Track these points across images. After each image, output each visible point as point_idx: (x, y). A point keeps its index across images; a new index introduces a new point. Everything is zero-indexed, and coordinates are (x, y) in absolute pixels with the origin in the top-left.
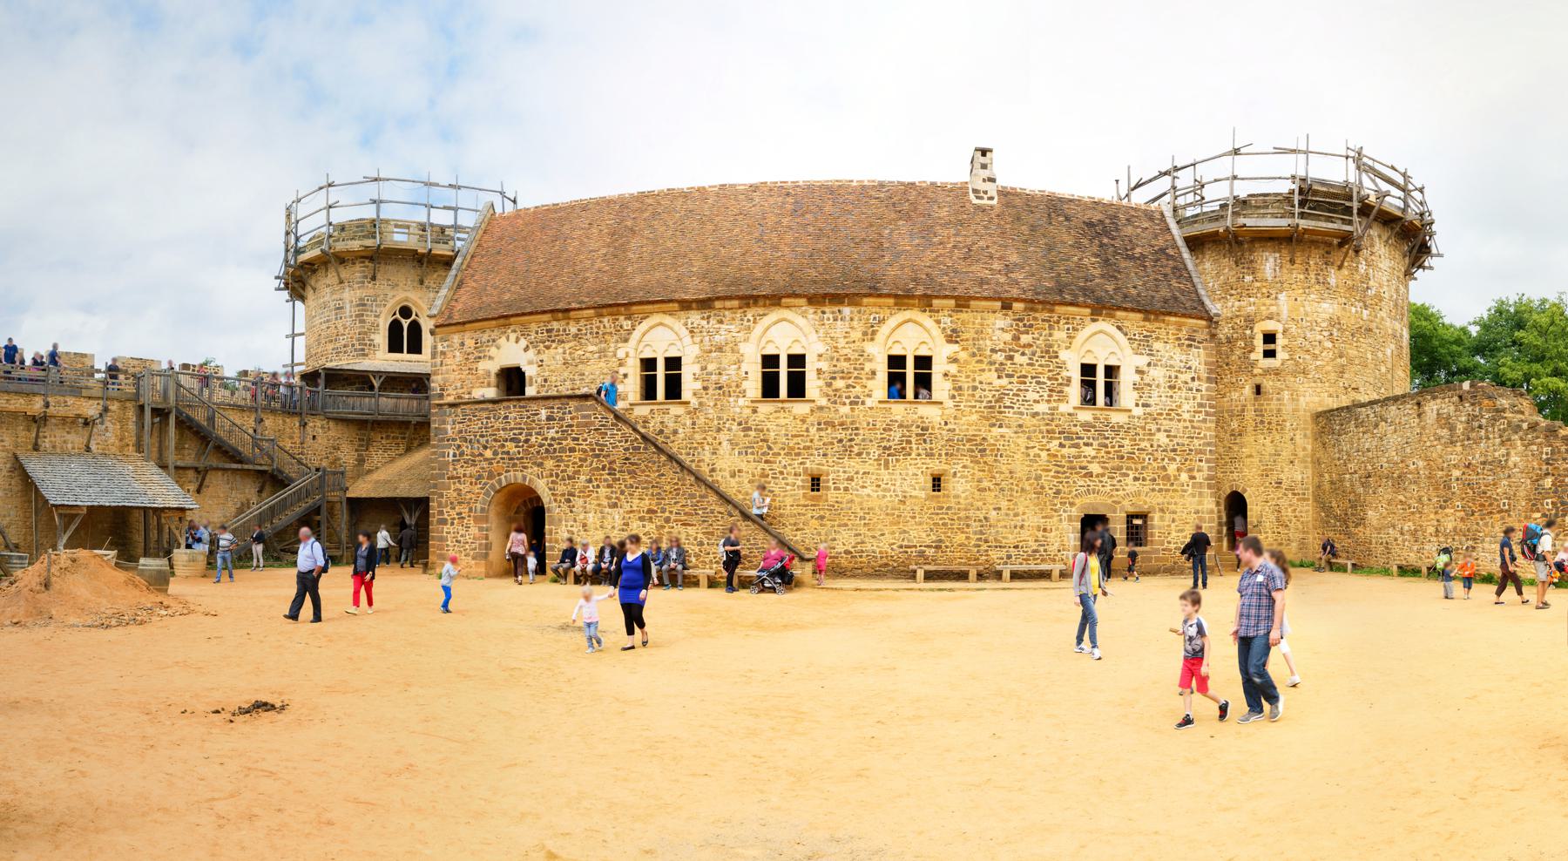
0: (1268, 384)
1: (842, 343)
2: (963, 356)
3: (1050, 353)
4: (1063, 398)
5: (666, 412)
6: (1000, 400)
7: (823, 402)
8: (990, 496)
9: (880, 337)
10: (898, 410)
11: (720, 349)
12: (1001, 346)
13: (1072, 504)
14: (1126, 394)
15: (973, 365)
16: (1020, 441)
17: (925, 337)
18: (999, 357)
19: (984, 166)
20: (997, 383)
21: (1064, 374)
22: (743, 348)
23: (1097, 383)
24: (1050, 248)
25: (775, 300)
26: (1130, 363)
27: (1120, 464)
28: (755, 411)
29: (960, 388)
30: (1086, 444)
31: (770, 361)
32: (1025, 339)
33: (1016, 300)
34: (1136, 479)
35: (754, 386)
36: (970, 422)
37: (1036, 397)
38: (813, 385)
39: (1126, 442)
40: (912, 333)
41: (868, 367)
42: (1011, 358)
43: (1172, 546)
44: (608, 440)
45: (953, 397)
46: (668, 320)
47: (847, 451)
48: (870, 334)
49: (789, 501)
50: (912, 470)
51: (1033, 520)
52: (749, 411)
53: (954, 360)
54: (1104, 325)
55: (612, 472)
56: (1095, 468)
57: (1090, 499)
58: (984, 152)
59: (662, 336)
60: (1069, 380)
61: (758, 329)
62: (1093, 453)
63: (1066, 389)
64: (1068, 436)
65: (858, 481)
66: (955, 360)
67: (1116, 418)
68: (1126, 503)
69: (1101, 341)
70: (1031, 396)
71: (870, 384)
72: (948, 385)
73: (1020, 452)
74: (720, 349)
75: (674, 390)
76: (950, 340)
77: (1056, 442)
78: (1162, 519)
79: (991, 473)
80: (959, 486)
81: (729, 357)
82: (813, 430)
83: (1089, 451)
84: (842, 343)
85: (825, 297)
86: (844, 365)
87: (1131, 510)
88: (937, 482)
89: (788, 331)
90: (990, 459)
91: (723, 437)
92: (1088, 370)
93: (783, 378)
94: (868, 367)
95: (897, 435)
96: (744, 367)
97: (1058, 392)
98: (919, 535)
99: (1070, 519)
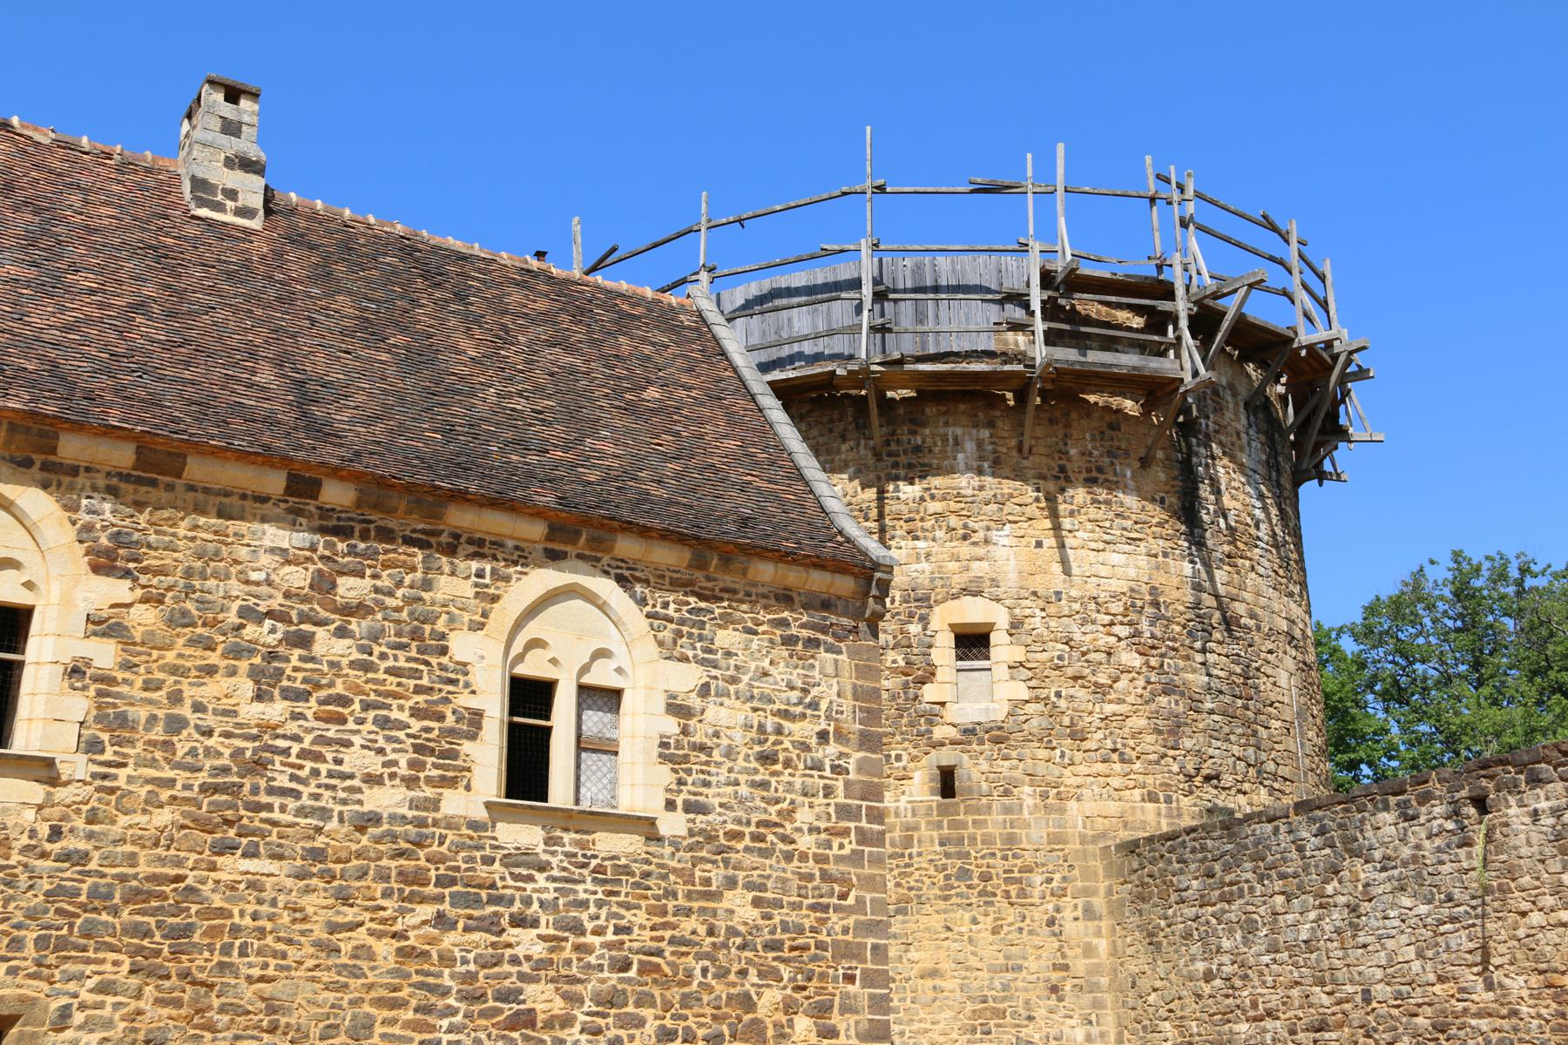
2: (144, 618)
6: (258, 765)
12: (277, 602)
16: (310, 903)
18: (265, 634)
20: (252, 712)
21: (464, 700)
29: (123, 721)
30: (519, 921)
32: (350, 588)
33: (336, 472)
37: (374, 764)
39: (641, 917)
42: (305, 641)
45: (94, 746)
56: (541, 998)
62: (539, 950)
63: (466, 747)
70: (357, 760)
72: (80, 705)
76: (104, 563)
77: (427, 911)
90: (202, 963)
97: (439, 758)
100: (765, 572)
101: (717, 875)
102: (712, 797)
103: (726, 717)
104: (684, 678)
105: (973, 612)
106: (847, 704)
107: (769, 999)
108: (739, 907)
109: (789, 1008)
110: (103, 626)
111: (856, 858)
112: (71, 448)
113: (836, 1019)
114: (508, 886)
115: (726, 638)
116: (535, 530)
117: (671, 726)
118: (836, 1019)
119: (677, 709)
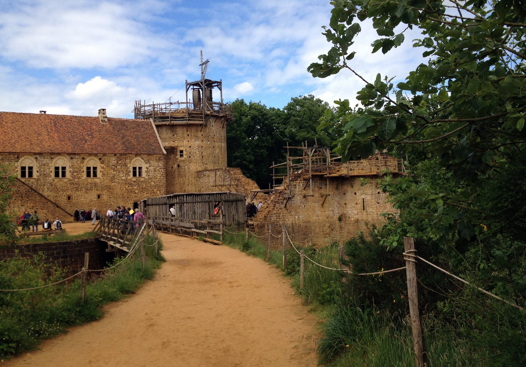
0: (181, 164)
1: (76, 164)
3: (125, 165)
4: (129, 175)
5: (30, 181)
6: (114, 177)
8: (112, 199)
9: (85, 163)
10: (89, 180)
11: (44, 165)
14: (144, 174)
15: (107, 169)
17: (96, 163)
19: (104, 114)
20: (113, 173)
22: (50, 165)
24: (123, 137)
25: (59, 154)
26: (144, 166)
27: (143, 190)
28: (54, 181)
31: (57, 168)
35: (53, 174)
36: (107, 182)
38: (68, 174)
40: (93, 162)
41: (82, 170)
44: (21, 189)
46: (30, 157)
47: (77, 190)
49: (63, 202)
52: (52, 181)
54: (139, 158)
55: (22, 197)
56: (137, 191)
57: (136, 199)
58: (104, 110)
59: (27, 162)
61: (54, 160)
64: (131, 184)
65: (80, 197)
66: (103, 168)
67: (142, 179)
69: (138, 162)
70: (121, 175)
71: (83, 174)
72: (101, 174)
74: (44, 165)
75: (31, 175)
80: (105, 197)
81: (46, 167)
82: (69, 185)
83: (135, 187)
84: (76, 164)
86: (76, 169)
88: (99, 196)
91: (46, 187)
92: (135, 168)
94: (82, 170)
95: (89, 186)
96: (51, 170)
97: (127, 174)
101: (150, 181)
104: (147, 165)
105: (181, 149)
107: (155, 190)
108: (153, 183)
115: (151, 161)
119: (147, 168)
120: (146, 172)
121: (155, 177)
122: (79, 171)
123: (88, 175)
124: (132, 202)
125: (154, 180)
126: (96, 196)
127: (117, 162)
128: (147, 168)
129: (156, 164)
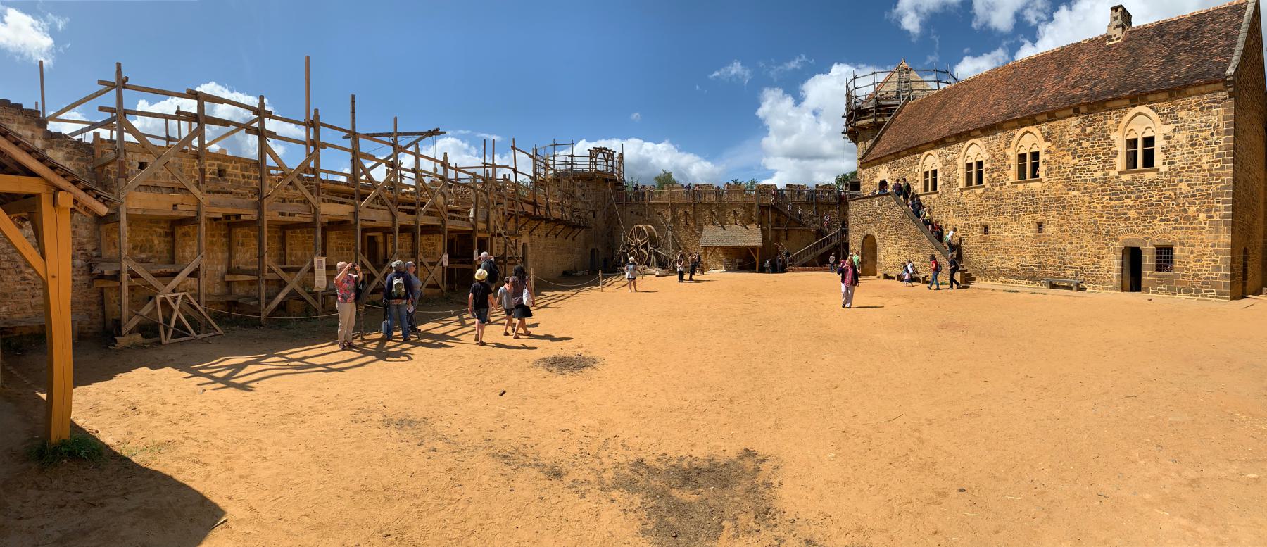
2: (1053, 148)
3: (1105, 136)
4: (1112, 167)
6: (1074, 173)
7: (988, 186)
9: (1013, 145)
13: (1117, 240)
17: (1035, 140)
20: (1072, 162)
21: (1114, 149)
23: (1142, 153)
27: (1150, 209)
32: (1089, 130)
34: (1162, 220)
35: (961, 182)
40: (1031, 139)
42: (1080, 144)
43: (1191, 273)
46: (931, 152)
47: (998, 213)
48: (1008, 145)
50: (1027, 221)
51: (1092, 250)
53: (1047, 152)
56: (1133, 214)
57: (1128, 236)
60: (1116, 153)
64: (1116, 193)
68: (1154, 238)
69: (1143, 121)
70: (1092, 167)
71: (1008, 173)
73: (1084, 205)
76: (1046, 140)
78: (1182, 250)
79: (1067, 218)
80: (1050, 229)
83: (1129, 202)
85: (988, 129)
87: (1158, 244)
88: (1040, 225)
89: (977, 150)
93: (975, 174)
95: (1020, 201)
98: (1030, 259)
99: (1115, 250)
100: (1192, 90)
101: (1177, 180)
102: (1176, 159)
103: (1182, 137)
104: (1168, 129)
106: (1221, 123)
107: (1192, 210)
108: (1184, 187)
109: (1198, 211)
110: (1047, 152)
111: (1222, 168)
112: (1038, 119)
113: (1213, 213)
114: (1125, 190)
115: (1181, 114)
116: (1127, 102)
117: (1165, 143)
118: (1213, 213)
119: (1167, 138)
120: (1164, 150)
121: (1194, 166)
122: (1001, 167)
123: (1022, 174)
124: (1118, 245)
125: (1187, 175)
126: (1034, 227)
127: (1084, 130)
128: (1167, 138)
129: (1199, 119)
